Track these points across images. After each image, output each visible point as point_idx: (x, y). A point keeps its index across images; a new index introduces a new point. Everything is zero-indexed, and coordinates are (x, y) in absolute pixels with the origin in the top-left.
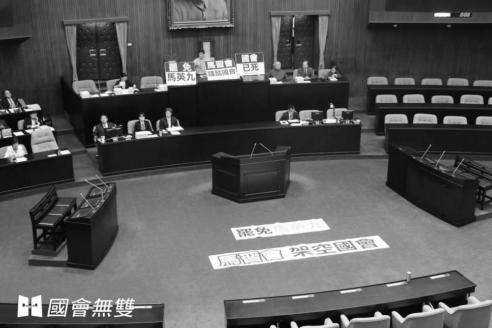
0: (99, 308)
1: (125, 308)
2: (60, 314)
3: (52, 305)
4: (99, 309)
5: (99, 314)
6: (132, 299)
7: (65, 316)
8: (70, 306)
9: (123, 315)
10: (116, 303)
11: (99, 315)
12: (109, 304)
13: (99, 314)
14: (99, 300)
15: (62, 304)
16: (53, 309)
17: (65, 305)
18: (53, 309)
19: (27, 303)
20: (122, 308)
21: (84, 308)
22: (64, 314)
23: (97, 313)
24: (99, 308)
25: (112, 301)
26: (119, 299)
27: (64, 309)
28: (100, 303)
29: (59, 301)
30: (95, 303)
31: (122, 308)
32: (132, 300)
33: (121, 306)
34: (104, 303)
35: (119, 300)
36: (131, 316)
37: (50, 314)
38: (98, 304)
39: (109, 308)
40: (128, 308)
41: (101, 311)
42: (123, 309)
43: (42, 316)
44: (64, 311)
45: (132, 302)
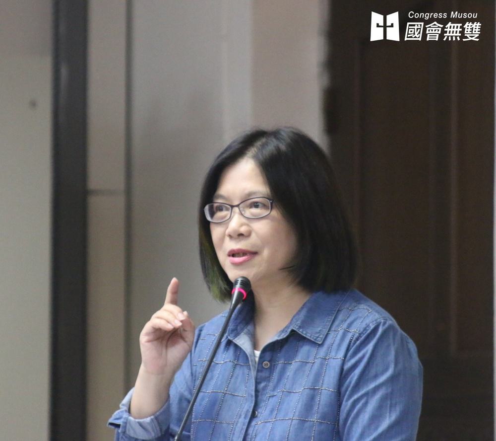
0: (450, 31)
1: (472, 31)
2: (415, 37)
3: (409, 29)
4: (450, 33)
5: (450, 38)
6: (479, 23)
7: (420, 39)
8: (425, 29)
9: (470, 39)
10: (464, 27)
11: (450, 39)
12: (459, 27)
13: (450, 38)
14: (450, 24)
15: (418, 27)
16: (410, 33)
17: (420, 29)
18: (410, 33)
21: (436, 32)
22: (419, 37)
23: (448, 36)
24: (450, 31)
25: (461, 25)
26: (468, 23)
27: (419, 33)
28: (451, 27)
29: (414, 25)
30: (446, 27)
32: (479, 24)
33: (469, 30)
34: (454, 26)
36: (477, 40)
38: (449, 28)
39: (458, 32)
40: (475, 31)
41: (451, 34)
42: (471, 33)
43: (399, 40)
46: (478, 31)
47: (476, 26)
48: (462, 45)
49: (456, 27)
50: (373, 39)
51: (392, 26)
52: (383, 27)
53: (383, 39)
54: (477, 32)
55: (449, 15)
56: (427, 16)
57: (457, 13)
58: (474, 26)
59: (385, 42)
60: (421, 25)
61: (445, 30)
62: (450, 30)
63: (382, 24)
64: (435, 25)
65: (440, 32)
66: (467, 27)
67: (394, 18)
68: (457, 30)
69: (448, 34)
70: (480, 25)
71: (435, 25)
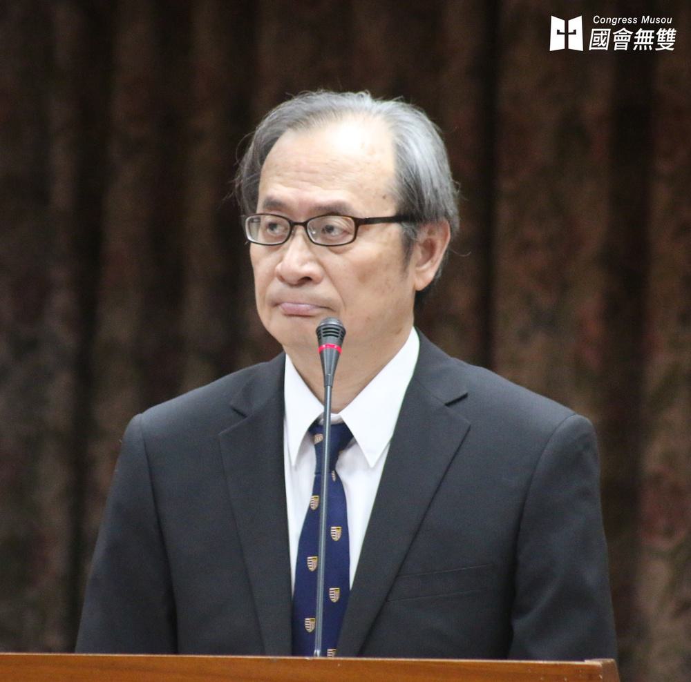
0: (641, 39)
1: (666, 39)
2: (601, 46)
3: (594, 36)
4: (640, 41)
5: (641, 47)
7: (606, 49)
8: (612, 37)
9: (664, 48)
11: (641, 49)
12: (651, 34)
13: (641, 47)
14: (640, 31)
16: (595, 41)
17: (607, 36)
18: (595, 41)
21: (625, 40)
23: (639, 45)
24: (641, 39)
25: (653, 31)
27: (606, 41)
28: (641, 34)
29: (600, 32)
30: (637, 34)
32: (674, 31)
33: (663, 38)
34: (645, 33)
35: (660, 30)
36: (672, 49)
39: (650, 40)
41: (642, 43)
43: (582, 50)
48: (652, 56)
49: (647, 34)
50: (553, 48)
51: (574, 32)
52: (566, 34)
53: (563, 47)
55: (639, 20)
56: (614, 21)
57: (648, 17)
58: (668, 33)
59: (566, 52)
60: (607, 32)
61: (636, 37)
63: (563, 30)
65: (629, 40)
67: (576, 23)
69: (638, 43)
70: (675, 31)
71: (623, 31)
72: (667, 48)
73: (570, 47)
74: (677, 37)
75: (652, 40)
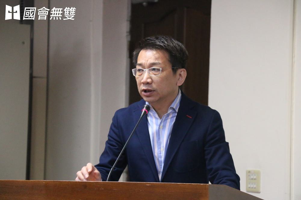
0: (54, 13)
1: (70, 13)
2: (31, 17)
3: (26, 12)
4: (54, 14)
5: (54, 18)
6: (74, 8)
7: (34, 19)
8: (37, 12)
9: (68, 18)
10: (64, 10)
11: (54, 19)
12: (60, 11)
13: (54, 18)
14: (54, 9)
15: (32, 11)
16: (26, 14)
17: (34, 12)
18: (26, 14)
19: (11, 11)
20: (68, 13)
21: (45, 14)
22: (33, 18)
23: (53, 17)
24: (54, 13)
25: (62, 9)
26: (66, 8)
27: (33, 14)
28: (55, 10)
29: (30, 9)
30: (52, 10)
31: (68, 13)
32: (74, 8)
33: (68, 13)
34: (57, 10)
35: (66, 8)
36: (73, 19)
37: (25, 18)
39: (60, 14)
40: (72, 13)
41: (55, 15)
42: (69, 14)
43: (20, 19)
44: (33, 16)
45: (74, 10)
46: (74, 13)
47: (72, 10)
48: (62, 22)
54: (73, 14)
58: (71, 10)
61: (51, 12)
62: (54, 12)
64: (44, 9)
65: (47, 14)
66: (66, 11)
68: (59, 12)
69: (53, 15)
70: (75, 9)
71: (44, 9)
72: (70, 18)
73: (14, 18)
74: (76, 12)
75: (61, 14)
